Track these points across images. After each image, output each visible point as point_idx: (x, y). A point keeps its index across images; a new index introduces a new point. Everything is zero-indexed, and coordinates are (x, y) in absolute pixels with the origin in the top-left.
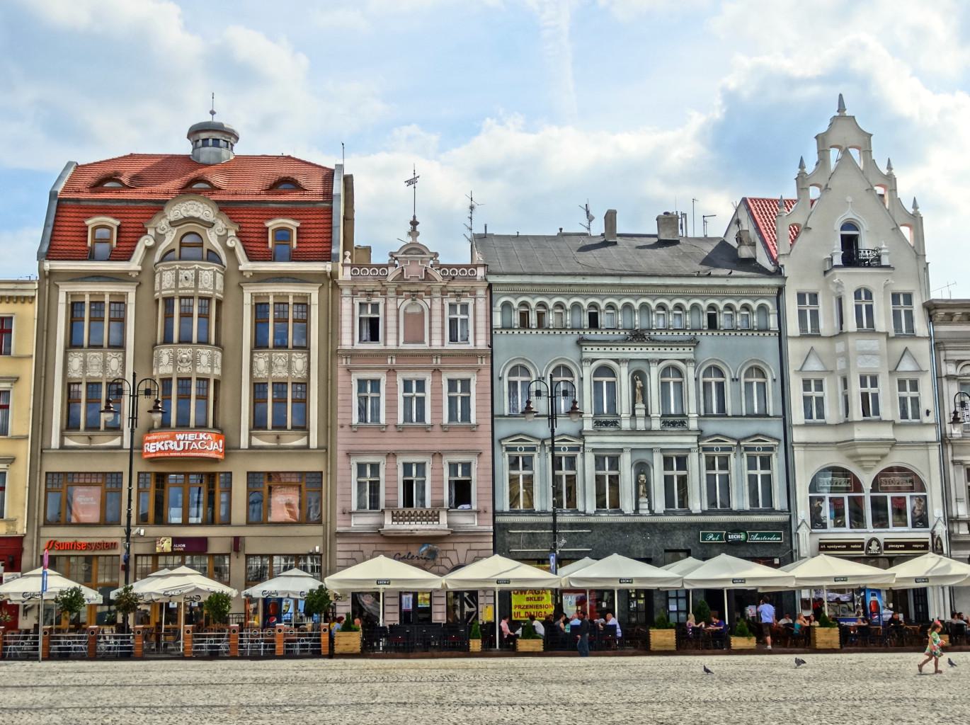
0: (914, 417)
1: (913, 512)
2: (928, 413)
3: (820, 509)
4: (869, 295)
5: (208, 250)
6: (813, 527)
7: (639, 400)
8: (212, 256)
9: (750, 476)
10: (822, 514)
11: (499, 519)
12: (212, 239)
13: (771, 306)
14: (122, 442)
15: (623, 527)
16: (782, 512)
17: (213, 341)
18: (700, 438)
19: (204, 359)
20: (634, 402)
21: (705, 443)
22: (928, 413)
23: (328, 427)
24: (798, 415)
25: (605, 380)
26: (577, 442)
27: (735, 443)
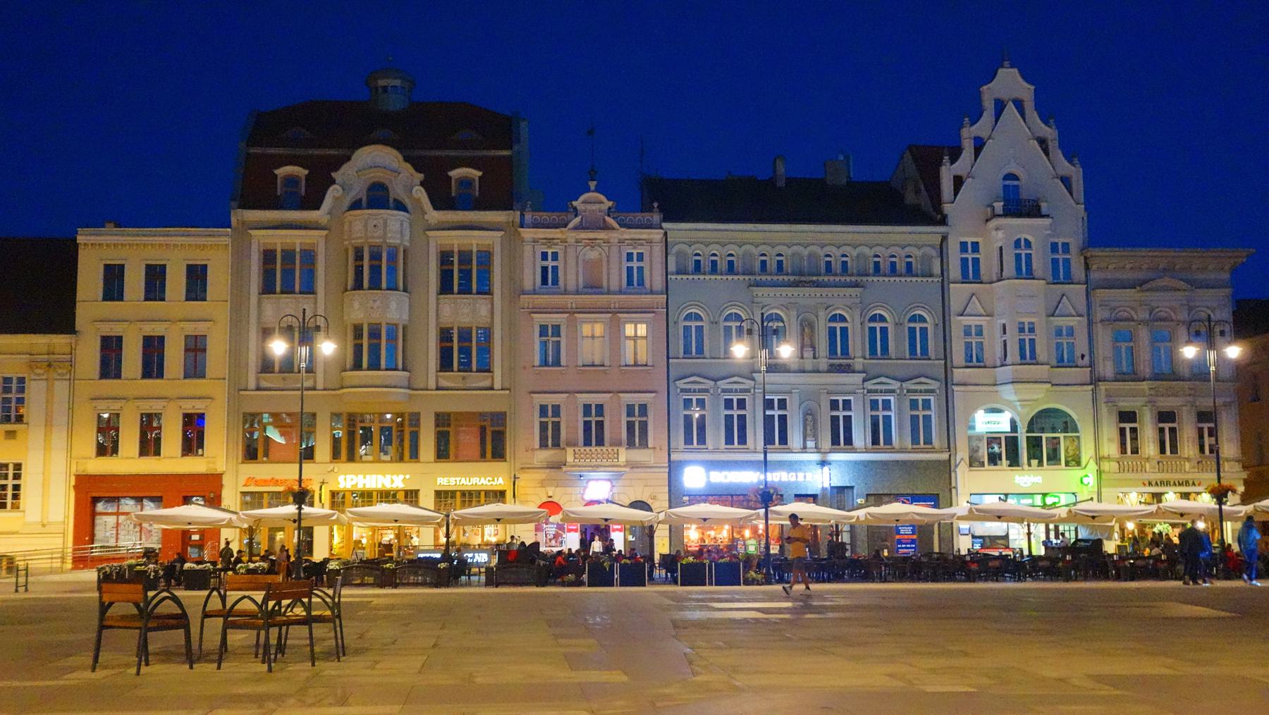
1: (1066, 451)
2: (1083, 356)
5: (395, 200)
8: (400, 206)
9: (912, 417)
10: (980, 454)
12: (397, 191)
13: (934, 253)
14: (315, 382)
17: (401, 287)
18: (865, 380)
19: (393, 305)
21: (869, 385)
22: (1083, 356)
23: (510, 371)
24: (958, 355)
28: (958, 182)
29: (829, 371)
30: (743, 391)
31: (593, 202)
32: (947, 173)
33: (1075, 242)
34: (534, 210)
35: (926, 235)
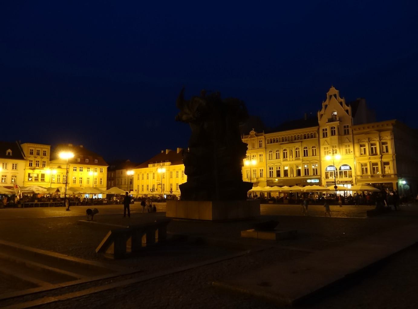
0: (349, 153)
2: (352, 152)
3: (328, 175)
4: (334, 128)
6: (326, 178)
7: (291, 154)
10: (328, 176)
11: (268, 179)
13: (316, 132)
15: (288, 180)
16: (319, 176)
18: (302, 162)
20: (290, 155)
21: (303, 162)
25: (285, 152)
26: (280, 164)
27: (309, 162)
28: (322, 115)
29: (295, 160)
30: (279, 165)
31: (253, 132)
32: (319, 114)
33: (350, 125)
34: (245, 135)
35: (314, 129)
